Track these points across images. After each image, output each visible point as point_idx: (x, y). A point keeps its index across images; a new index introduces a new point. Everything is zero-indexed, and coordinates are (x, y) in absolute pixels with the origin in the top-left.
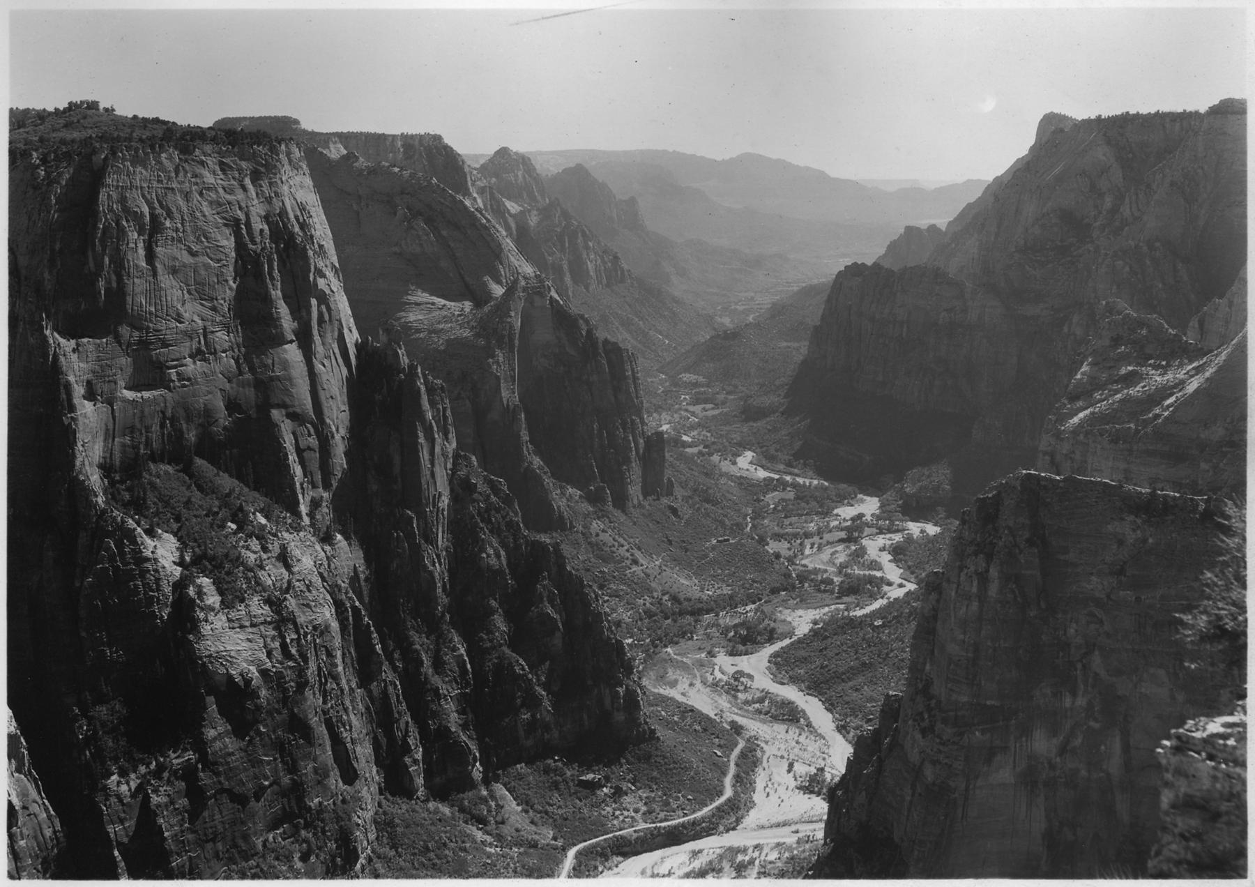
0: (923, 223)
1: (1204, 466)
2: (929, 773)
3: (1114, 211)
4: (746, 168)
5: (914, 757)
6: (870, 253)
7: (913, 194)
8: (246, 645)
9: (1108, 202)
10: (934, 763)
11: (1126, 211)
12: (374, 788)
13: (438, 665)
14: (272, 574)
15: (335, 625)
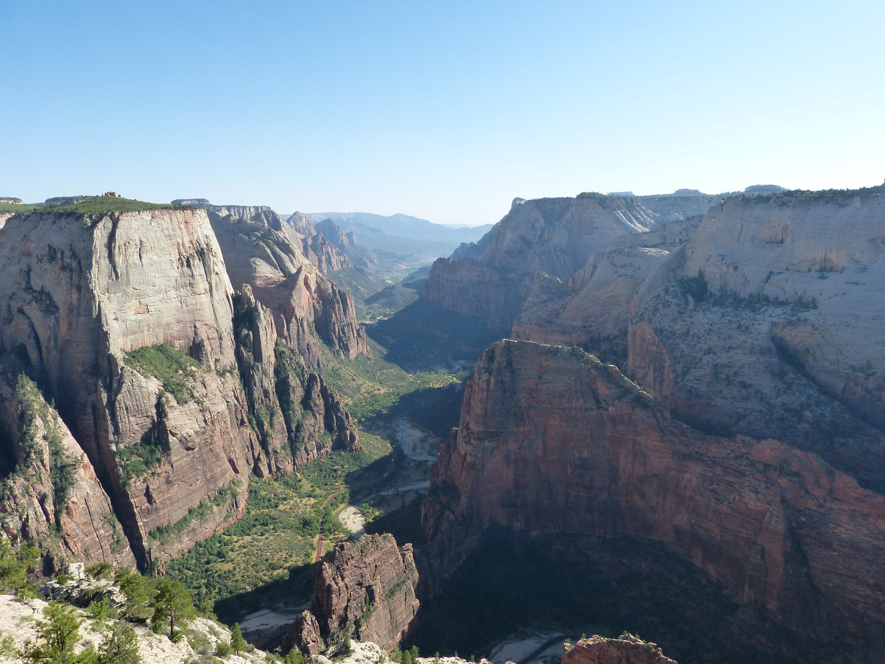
0: (468, 242)
1: (574, 335)
2: (469, 459)
3: (541, 236)
4: (397, 219)
5: (463, 453)
6: (447, 254)
7: (465, 230)
8: (188, 421)
9: (539, 232)
10: (471, 454)
11: (546, 236)
12: (246, 477)
13: (272, 425)
14: (199, 391)
15: (227, 412)
